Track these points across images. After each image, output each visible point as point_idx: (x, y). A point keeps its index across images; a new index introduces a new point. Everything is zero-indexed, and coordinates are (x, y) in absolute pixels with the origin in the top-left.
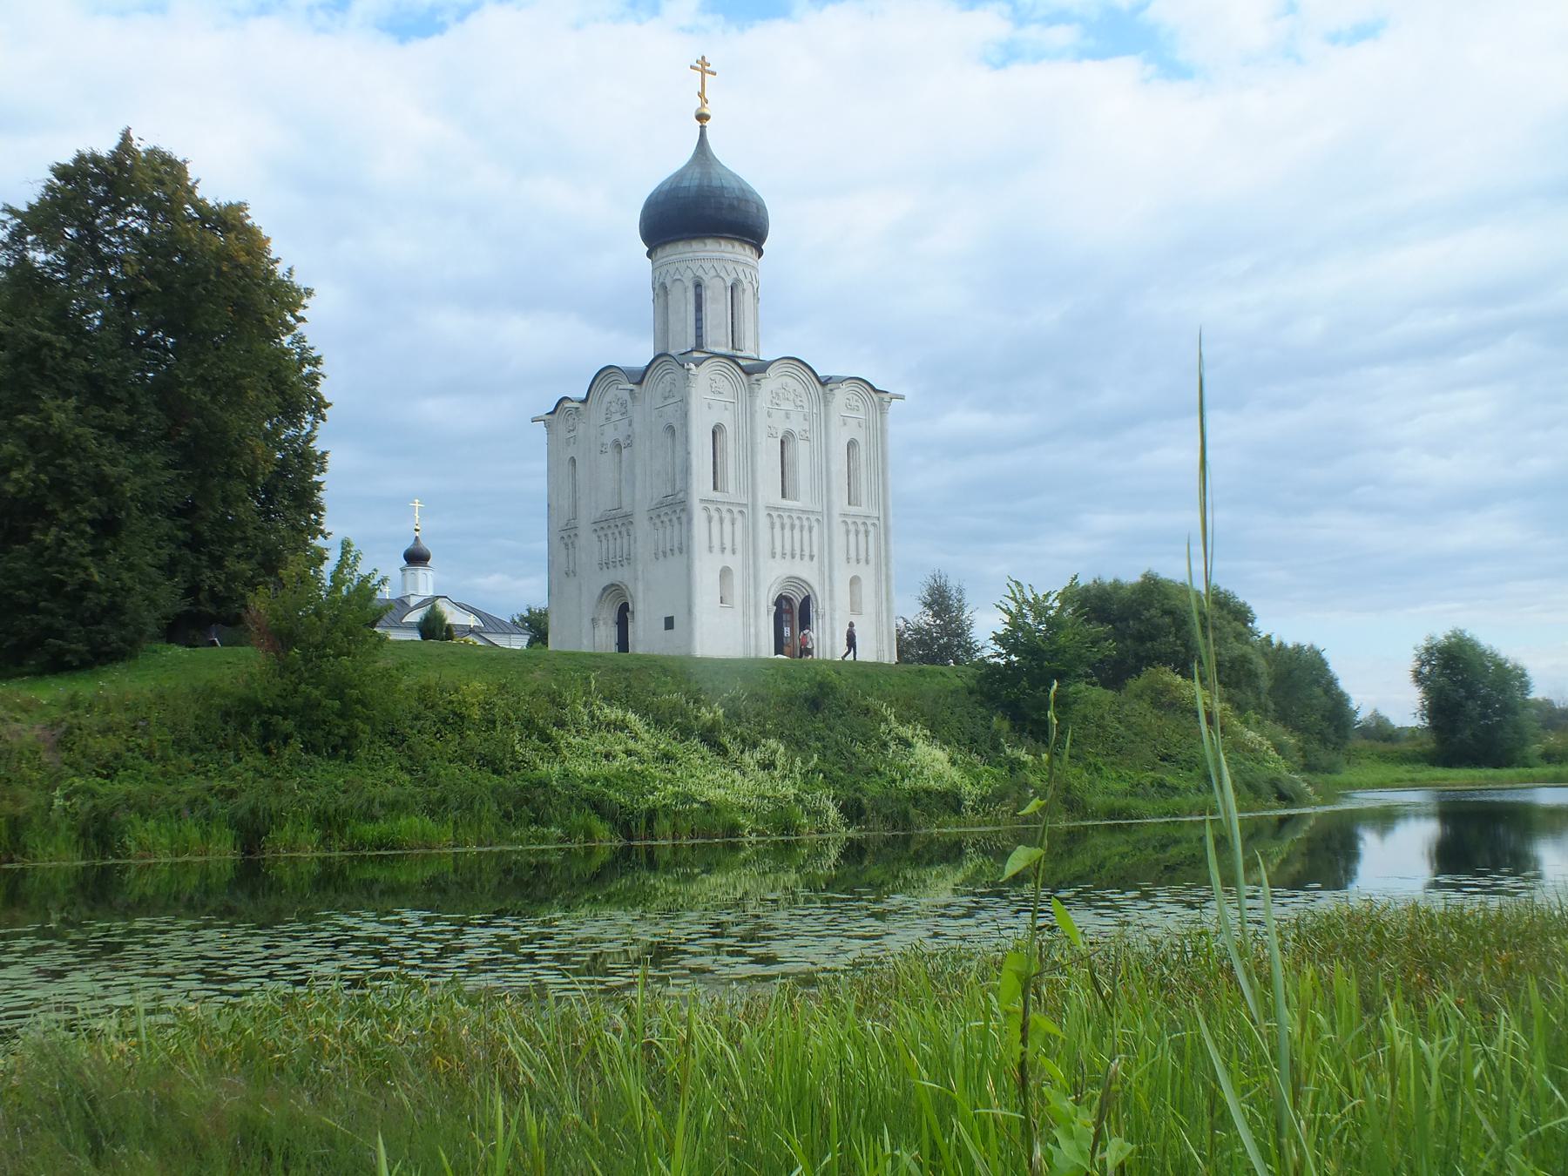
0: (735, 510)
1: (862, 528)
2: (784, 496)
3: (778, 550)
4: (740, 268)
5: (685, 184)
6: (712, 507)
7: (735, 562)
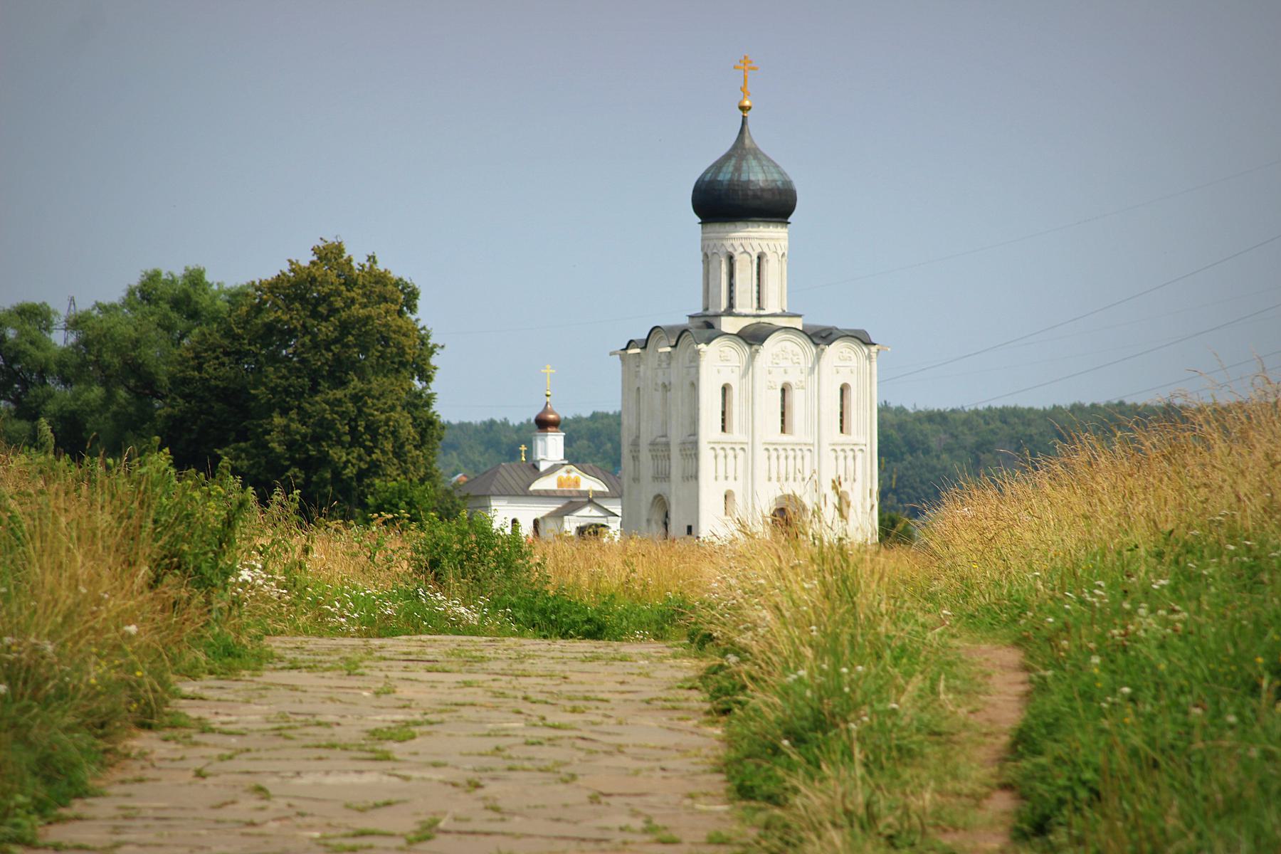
0: (737, 447)
1: (850, 454)
2: (783, 431)
3: (774, 476)
4: (764, 243)
5: (721, 177)
6: (717, 447)
7: (737, 488)
